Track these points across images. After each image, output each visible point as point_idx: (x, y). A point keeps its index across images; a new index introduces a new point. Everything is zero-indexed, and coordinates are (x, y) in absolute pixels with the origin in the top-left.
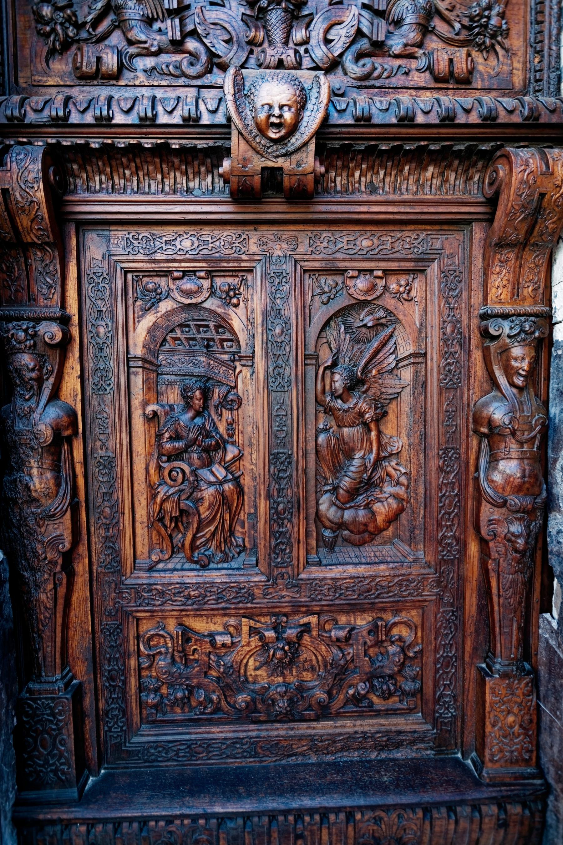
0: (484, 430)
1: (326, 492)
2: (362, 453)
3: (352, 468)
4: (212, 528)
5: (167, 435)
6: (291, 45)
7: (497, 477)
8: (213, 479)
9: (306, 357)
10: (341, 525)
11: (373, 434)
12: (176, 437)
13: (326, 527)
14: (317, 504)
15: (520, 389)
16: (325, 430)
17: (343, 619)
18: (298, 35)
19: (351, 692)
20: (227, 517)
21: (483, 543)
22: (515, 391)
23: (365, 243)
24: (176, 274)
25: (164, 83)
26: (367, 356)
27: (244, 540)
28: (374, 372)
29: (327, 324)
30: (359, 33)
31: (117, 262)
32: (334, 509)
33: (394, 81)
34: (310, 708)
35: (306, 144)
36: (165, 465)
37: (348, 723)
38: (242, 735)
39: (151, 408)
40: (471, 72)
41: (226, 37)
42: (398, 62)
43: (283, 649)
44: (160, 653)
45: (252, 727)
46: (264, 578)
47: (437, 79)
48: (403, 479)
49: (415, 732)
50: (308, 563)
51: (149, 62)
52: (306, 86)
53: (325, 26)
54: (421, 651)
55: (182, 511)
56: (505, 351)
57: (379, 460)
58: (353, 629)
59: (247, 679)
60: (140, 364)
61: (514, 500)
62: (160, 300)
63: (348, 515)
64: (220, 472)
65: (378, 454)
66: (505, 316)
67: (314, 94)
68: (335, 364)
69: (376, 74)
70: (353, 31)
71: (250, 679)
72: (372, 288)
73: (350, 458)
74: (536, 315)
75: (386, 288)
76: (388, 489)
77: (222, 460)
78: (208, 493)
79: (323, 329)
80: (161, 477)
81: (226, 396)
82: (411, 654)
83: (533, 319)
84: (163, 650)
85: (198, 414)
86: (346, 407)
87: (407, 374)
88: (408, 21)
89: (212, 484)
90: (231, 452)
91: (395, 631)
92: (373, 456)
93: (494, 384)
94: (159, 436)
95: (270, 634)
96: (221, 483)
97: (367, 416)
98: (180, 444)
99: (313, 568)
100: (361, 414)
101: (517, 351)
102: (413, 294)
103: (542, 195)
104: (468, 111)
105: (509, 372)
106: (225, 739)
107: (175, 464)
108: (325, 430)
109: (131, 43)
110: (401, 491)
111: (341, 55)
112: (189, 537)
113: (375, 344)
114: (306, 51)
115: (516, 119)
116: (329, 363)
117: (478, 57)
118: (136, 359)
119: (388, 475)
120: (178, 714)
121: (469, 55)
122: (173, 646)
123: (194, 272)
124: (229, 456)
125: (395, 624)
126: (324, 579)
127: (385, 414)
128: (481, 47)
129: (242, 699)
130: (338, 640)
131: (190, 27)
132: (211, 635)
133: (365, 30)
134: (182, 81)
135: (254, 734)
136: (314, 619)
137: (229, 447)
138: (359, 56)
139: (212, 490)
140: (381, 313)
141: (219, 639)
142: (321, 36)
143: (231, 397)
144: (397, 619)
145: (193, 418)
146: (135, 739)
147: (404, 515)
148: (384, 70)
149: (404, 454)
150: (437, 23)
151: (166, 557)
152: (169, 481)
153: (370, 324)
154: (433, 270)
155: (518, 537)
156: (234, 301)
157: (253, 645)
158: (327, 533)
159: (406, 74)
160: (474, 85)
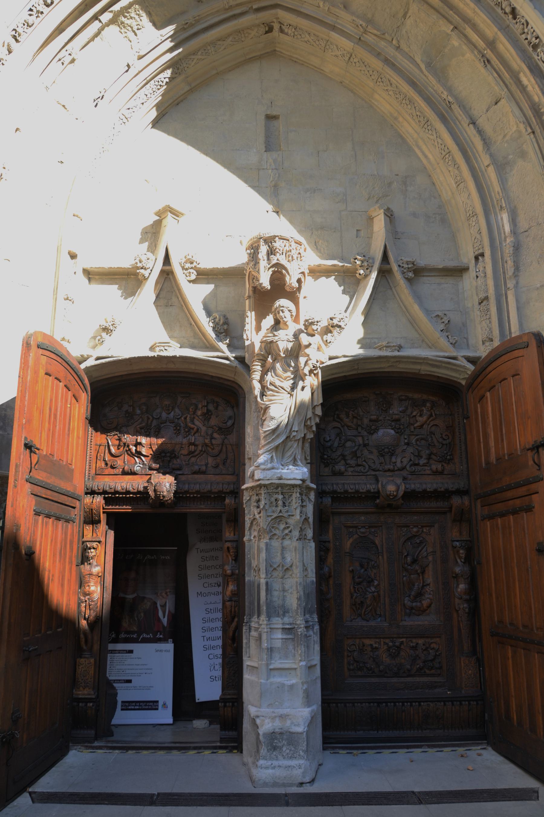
0: (454, 575)
1: (407, 596)
2: (417, 584)
3: (415, 588)
4: (371, 608)
5: (357, 577)
6: (391, 463)
7: (459, 590)
8: (371, 591)
9: (399, 552)
10: (412, 608)
11: (421, 577)
12: (359, 577)
13: (407, 609)
14: (404, 601)
15: (464, 563)
16: (405, 576)
17: (414, 640)
18: (393, 460)
19: (418, 666)
20: (375, 604)
21: (457, 611)
22: (462, 564)
23: (416, 518)
24: (359, 527)
25: (356, 474)
26: (418, 552)
27: (381, 613)
28: (420, 557)
29: (405, 542)
30: (411, 460)
31: (343, 524)
32: (409, 602)
33: (421, 473)
34: (404, 672)
35: (399, 499)
36: (356, 587)
37: (418, 678)
38: (381, 681)
39: (351, 569)
40: (443, 470)
41: (373, 461)
42: (422, 467)
43: (395, 649)
44: (354, 650)
45: (385, 679)
46: (388, 624)
47: (433, 472)
48: (432, 592)
49: (440, 682)
50: (402, 621)
51: (352, 469)
52: (399, 484)
53: (400, 459)
54: (441, 653)
55: (361, 602)
56: (458, 552)
57: (423, 586)
58: (417, 644)
59: (383, 662)
60: (348, 554)
61: (465, 597)
62: (354, 535)
63: (414, 604)
64: (373, 589)
65: (423, 584)
66: (457, 541)
67: (401, 487)
68: (408, 555)
69: (416, 471)
70: (409, 460)
71: (384, 662)
72: (417, 532)
73: (414, 585)
74: (466, 541)
75: (422, 531)
76: (427, 596)
77: (373, 585)
78: (369, 596)
79: (403, 544)
80: (355, 591)
81: (374, 565)
82: (438, 654)
83: (465, 542)
84: (355, 649)
85: (366, 570)
86: (412, 568)
87: (430, 558)
88: (424, 457)
89: (371, 593)
90: (376, 583)
91: (432, 646)
92: (421, 585)
93: (457, 562)
94: (353, 577)
95: (391, 644)
96: (374, 592)
97: (419, 571)
98: (360, 580)
99: (404, 622)
100: (417, 571)
101: (461, 551)
102: (431, 533)
103: (463, 509)
104: (441, 488)
105: (460, 558)
106: (376, 682)
107: (359, 586)
108: (405, 576)
109: (347, 464)
110: (431, 596)
111: (406, 466)
112: (364, 610)
113: (420, 549)
114: (396, 465)
115: (454, 489)
116: (406, 554)
117: (445, 465)
118: (347, 553)
119: (427, 591)
120: (359, 673)
121: (442, 465)
122: (359, 648)
123: (365, 527)
124: (376, 584)
125: (432, 643)
126: (407, 625)
127: (424, 571)
128: (445, 463)
129: (382, 668)
130: (413, 647)
131: (363, 459)
132: (371, 645)
133: (412, 459)
134: (361, 474)
135: (386, 681)
136: (404, 640)
137: (375, 581)
138: (411, 466)
139: (371, 594)
140: (421, 539)
141: (374, 645)
142: (400, 461)
143: (375, 565)
144: (432, 641)
145: (364, 571)
146: (346, 682)
147: (433, 605)
148: (418, 470)
149: (431, 585)
150: (433, 456)
151: (356, 618)
152: (357, 591)
153: (418, 542)
154: (436, 526)
155: (466, 608)
156: (376, 535)
157: (385, 648)
158: (408, 611)
159: (425, 471)
160: (444, 473)
